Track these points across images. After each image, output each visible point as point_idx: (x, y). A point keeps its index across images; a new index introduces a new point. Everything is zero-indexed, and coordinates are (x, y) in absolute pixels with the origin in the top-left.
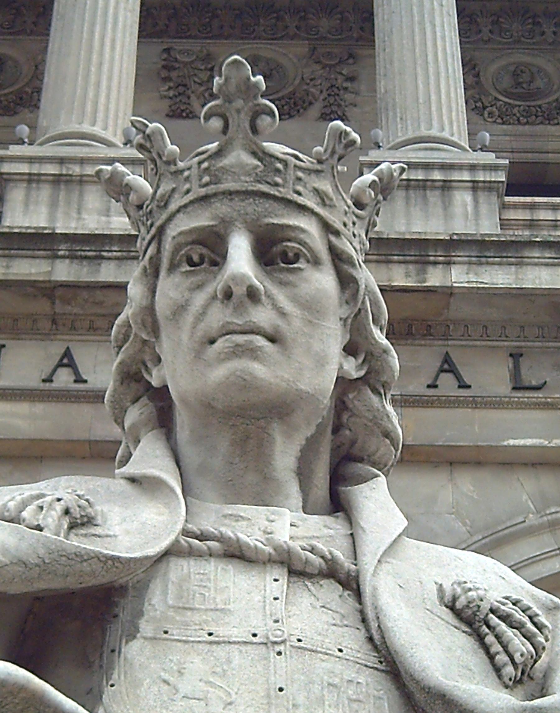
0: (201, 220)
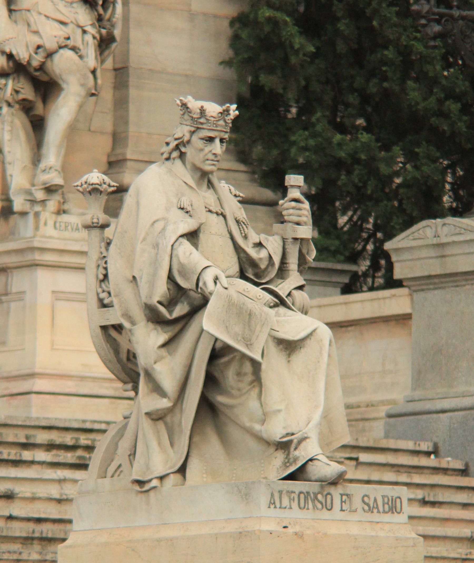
0: (212, 134)
